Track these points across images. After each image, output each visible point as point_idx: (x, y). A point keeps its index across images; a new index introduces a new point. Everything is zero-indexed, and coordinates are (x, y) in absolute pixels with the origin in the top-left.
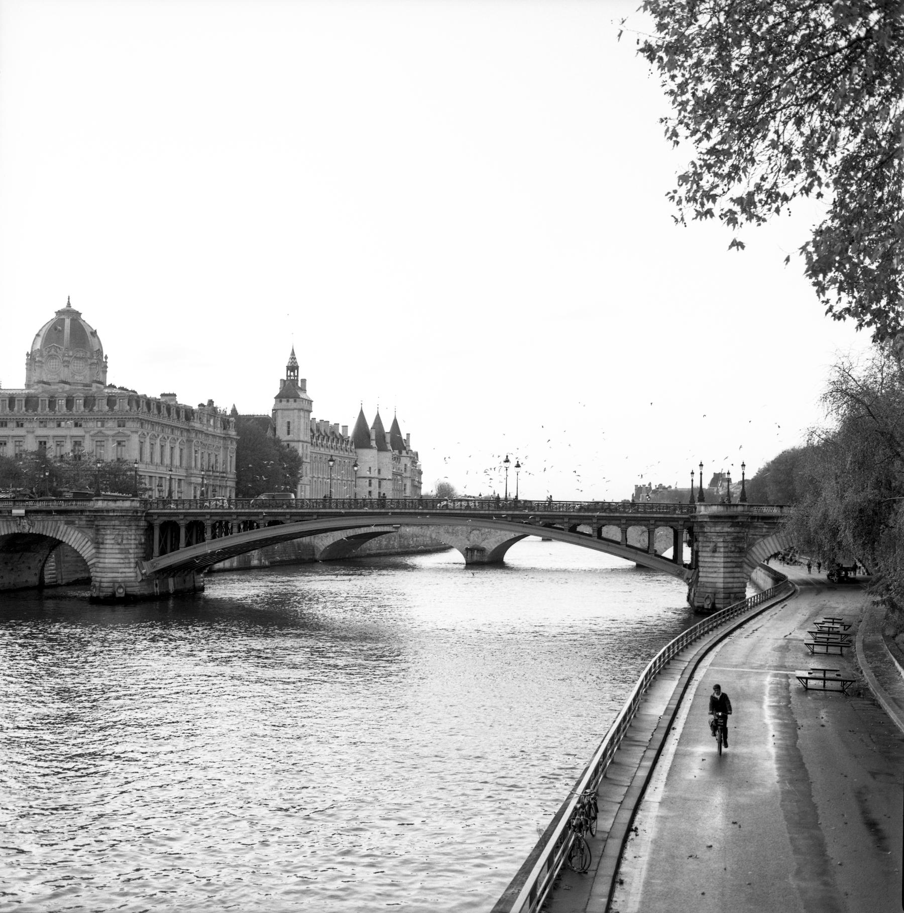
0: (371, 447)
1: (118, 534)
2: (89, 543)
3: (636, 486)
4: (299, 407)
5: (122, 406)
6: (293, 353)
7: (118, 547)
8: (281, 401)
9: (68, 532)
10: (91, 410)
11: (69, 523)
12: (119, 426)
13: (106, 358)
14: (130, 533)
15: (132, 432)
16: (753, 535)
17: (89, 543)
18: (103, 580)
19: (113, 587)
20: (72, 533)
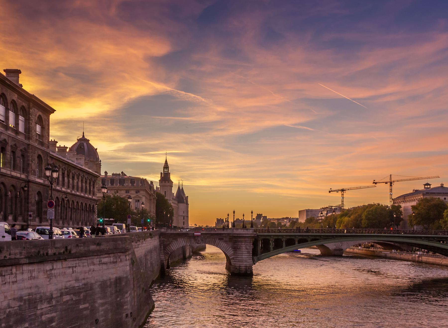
0: (185, 203)
1: (247, 245)
2: (230, 249)
3: (217, 219)
4: (170, 185)
5: (128, 184)
7: (246, 250)
8: (162, 182)
9: (220, 244)
10: (123, 185)
11: (220, 239)
12: (136, 193)
13: (100, 161)
14: (250, 244)
15: (143, 196)
17: (230, 249)
18: (241, 265)
19: (246, 269)
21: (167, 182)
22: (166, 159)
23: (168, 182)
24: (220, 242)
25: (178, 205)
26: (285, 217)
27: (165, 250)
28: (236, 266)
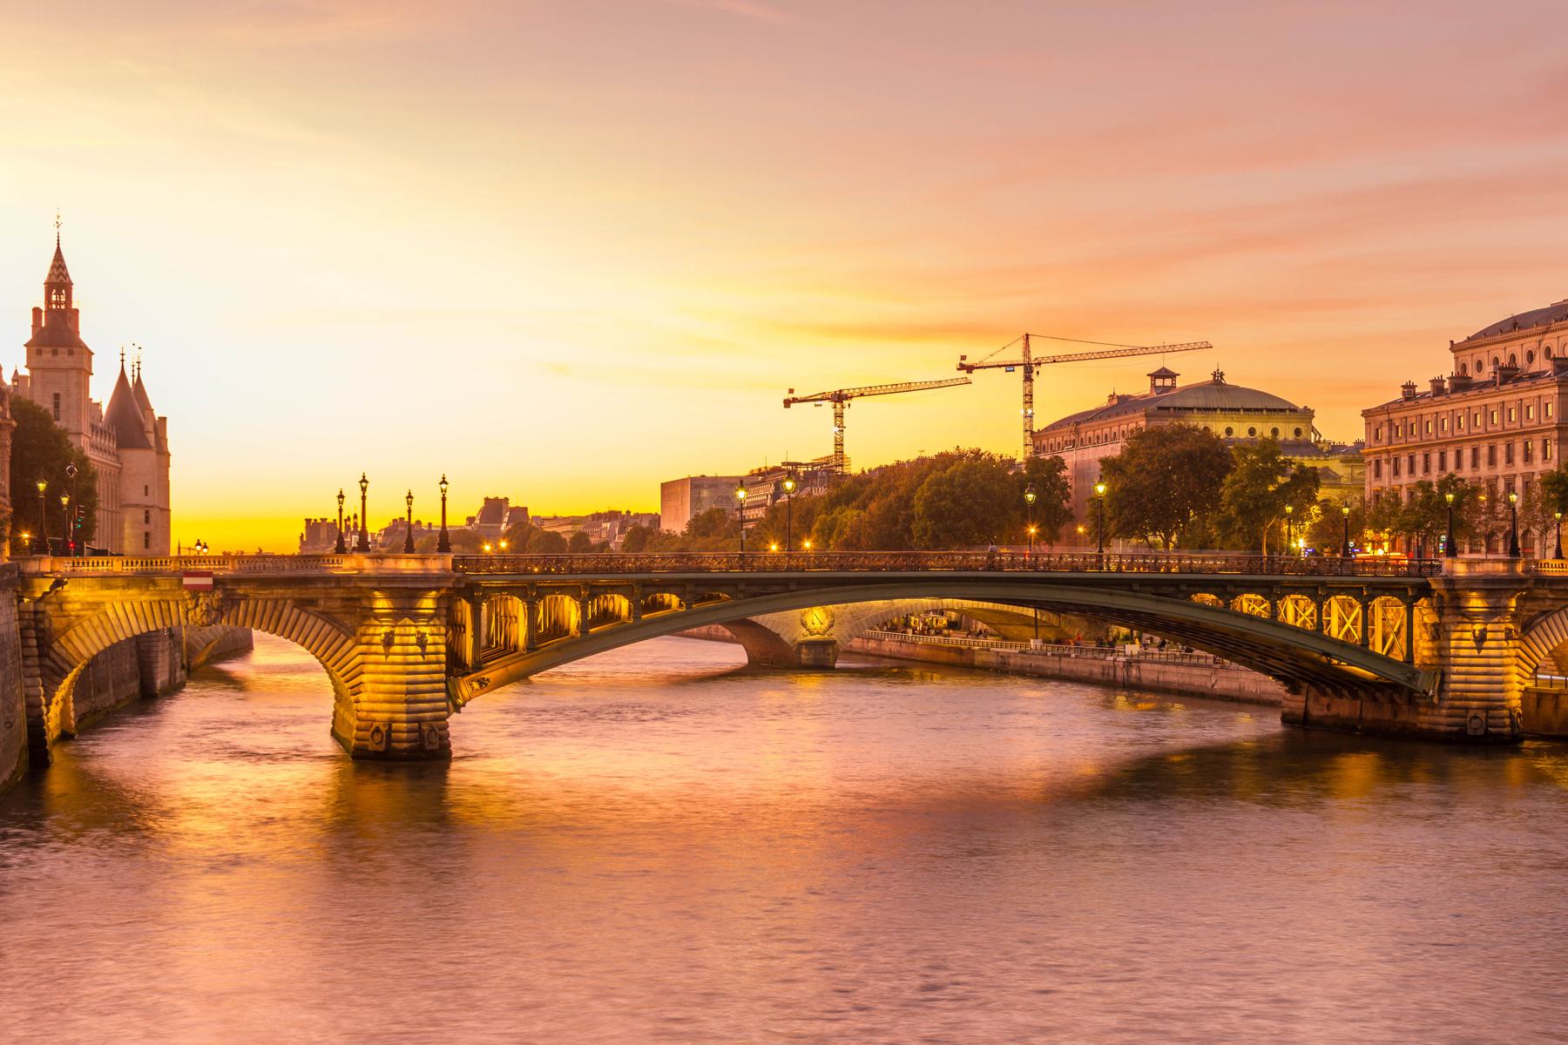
0: (149, 447)
3: (308, 521)
6: (59, 255)
8: (39, 352)
11: (303, 604)
16: (1529, 611)
20: (310, 623)
21: (65, 350)
22: (58, 248)
23: (71, 353)
24: (303, 617)
25: (118, 457)
26: (603, 510)
27: (48, 656)
28: (375, 721)
